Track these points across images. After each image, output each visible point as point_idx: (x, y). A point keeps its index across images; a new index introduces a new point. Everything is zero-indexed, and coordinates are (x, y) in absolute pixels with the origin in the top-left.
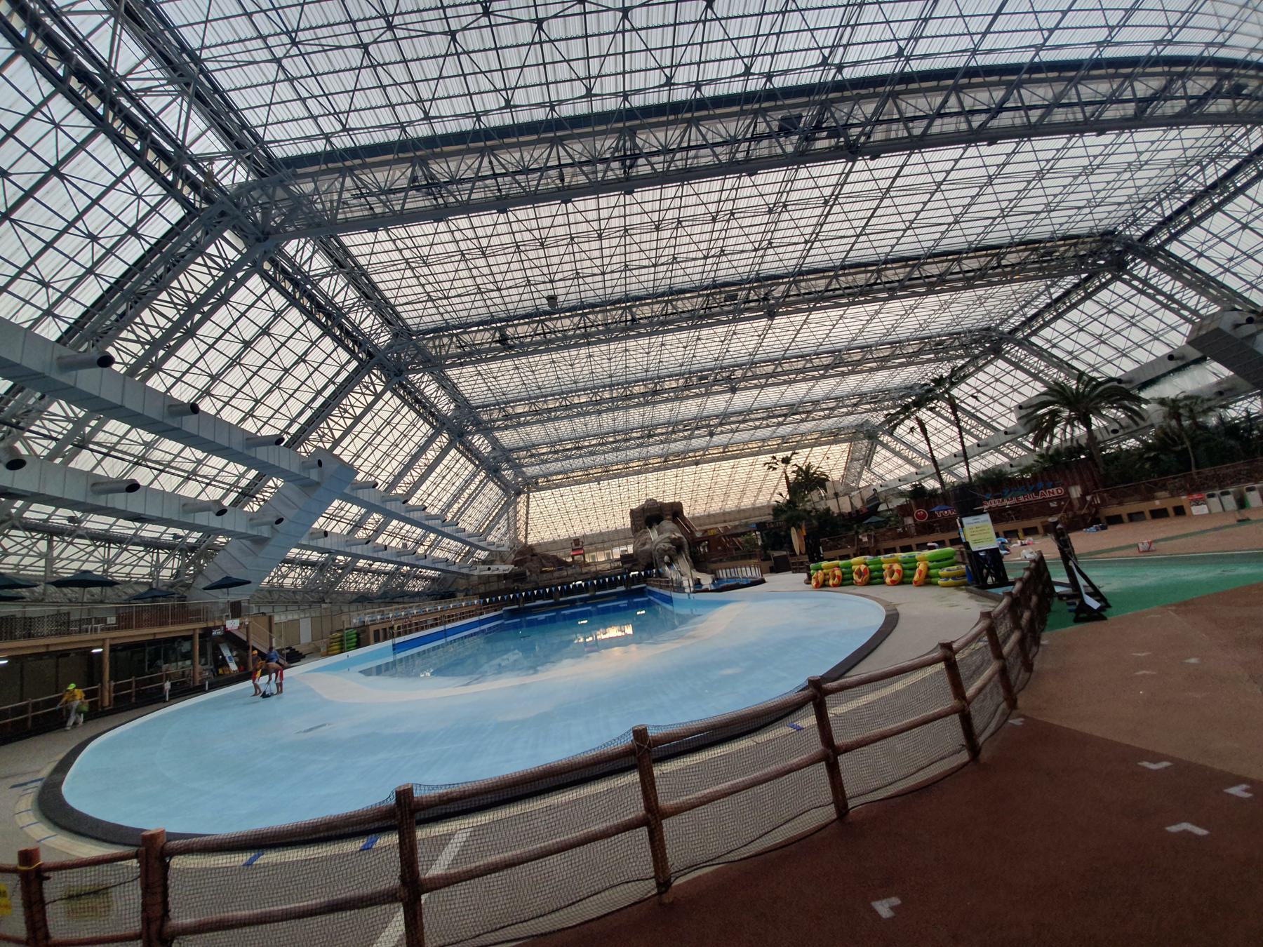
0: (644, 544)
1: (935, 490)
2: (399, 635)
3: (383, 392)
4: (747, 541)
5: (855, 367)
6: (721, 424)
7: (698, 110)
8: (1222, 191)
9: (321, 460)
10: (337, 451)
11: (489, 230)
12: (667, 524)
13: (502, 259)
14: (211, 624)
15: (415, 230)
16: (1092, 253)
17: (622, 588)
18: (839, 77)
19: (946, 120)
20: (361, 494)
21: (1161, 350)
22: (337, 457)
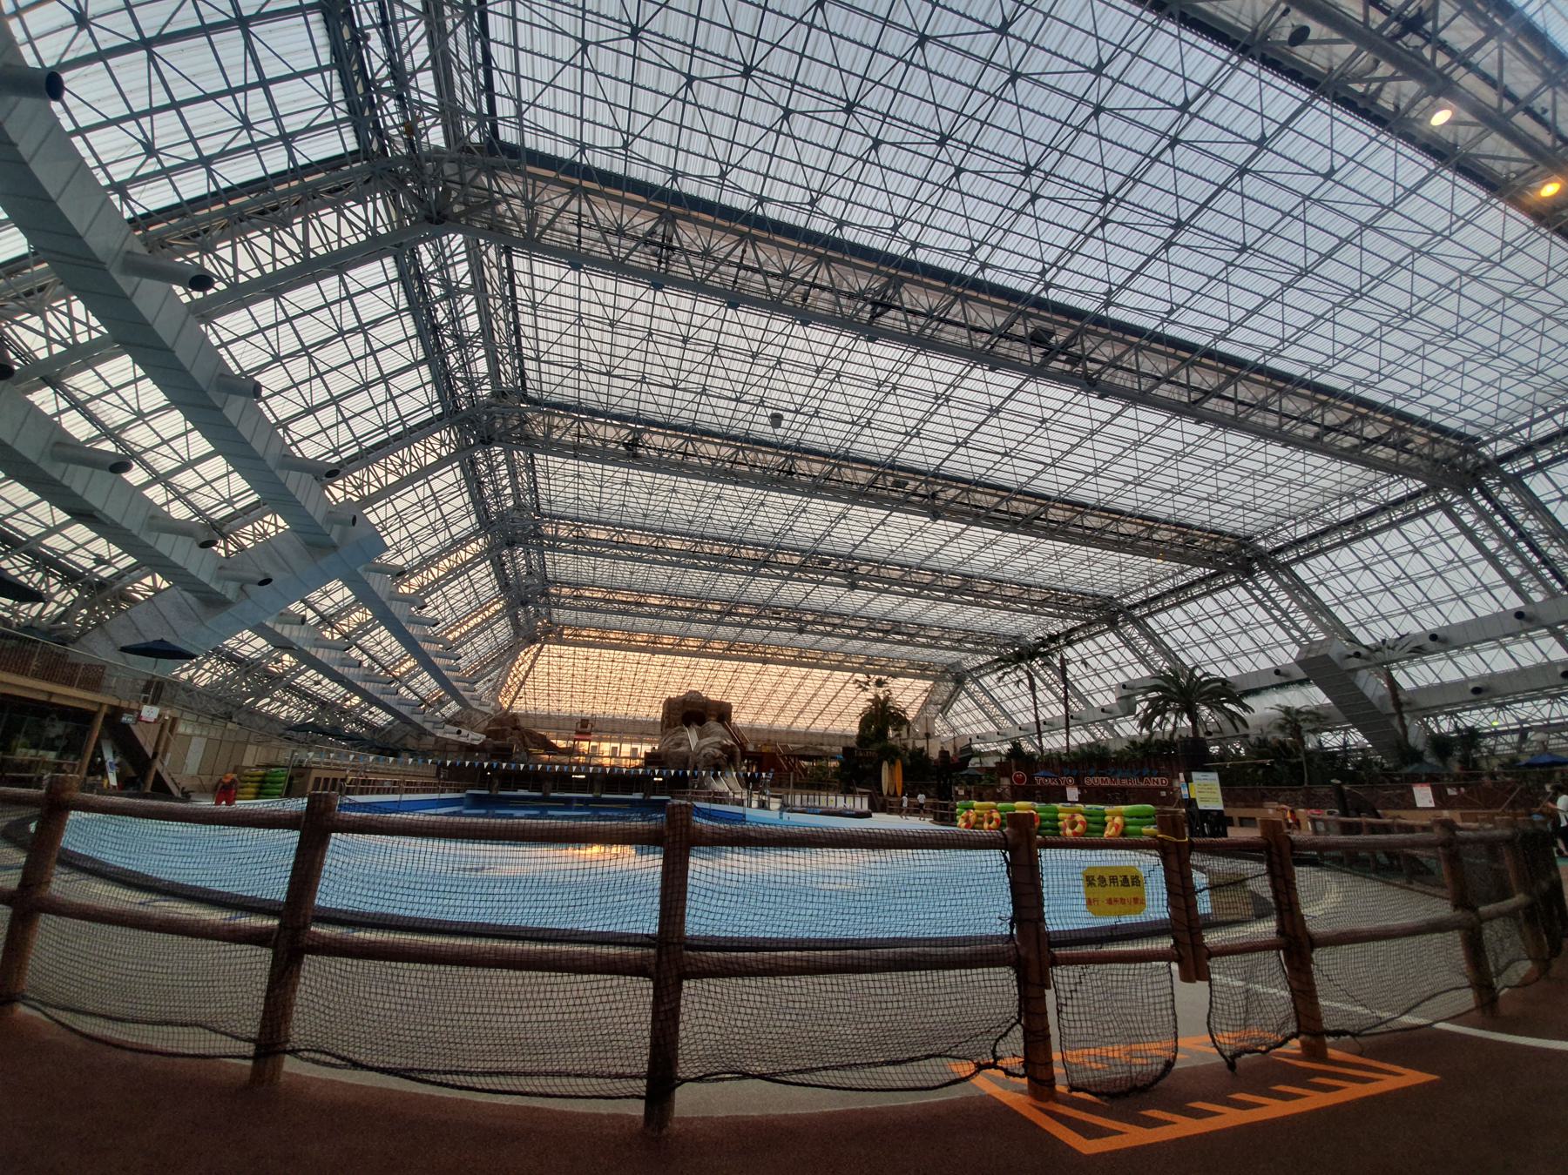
0: (679, 745)
1: (1033, 754)
4: (819, 768)
5: (981, 599)
7: (903, 269)
8: (1357, 529)
9: (352, 515)
11: (549, 285)
12: (712, 724)
13: (555, 326)
14: (124, 704)
15: (626, 289)
16: (1227, 552)
17: (638, 796)
18: (1043, 295)
19: (1120, 373)
21: (1264, 664)
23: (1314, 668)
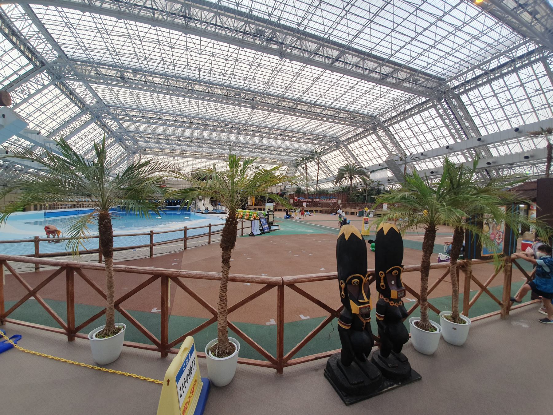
2: (50, 209)
3: (49, 85)
6: (235, 146)
8: (406, 114)
10: (17, 110)
20: (30, 136)
22: (17, 115)
23: (390, 164)
